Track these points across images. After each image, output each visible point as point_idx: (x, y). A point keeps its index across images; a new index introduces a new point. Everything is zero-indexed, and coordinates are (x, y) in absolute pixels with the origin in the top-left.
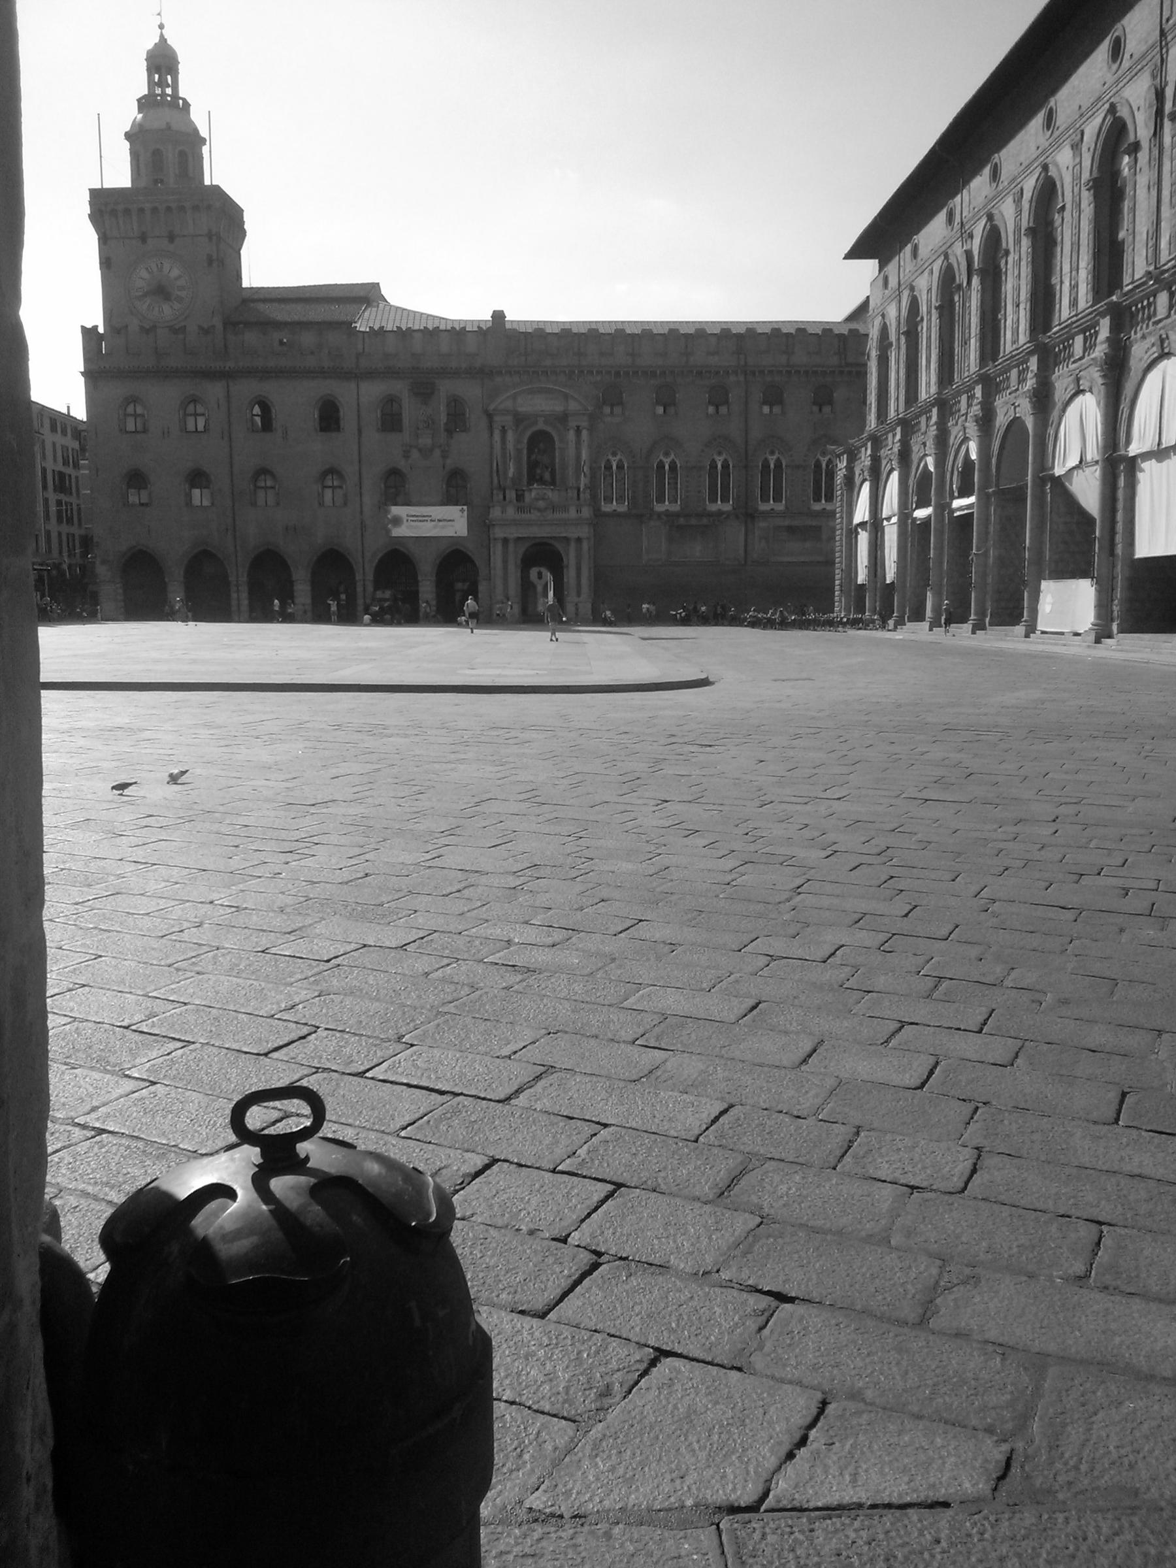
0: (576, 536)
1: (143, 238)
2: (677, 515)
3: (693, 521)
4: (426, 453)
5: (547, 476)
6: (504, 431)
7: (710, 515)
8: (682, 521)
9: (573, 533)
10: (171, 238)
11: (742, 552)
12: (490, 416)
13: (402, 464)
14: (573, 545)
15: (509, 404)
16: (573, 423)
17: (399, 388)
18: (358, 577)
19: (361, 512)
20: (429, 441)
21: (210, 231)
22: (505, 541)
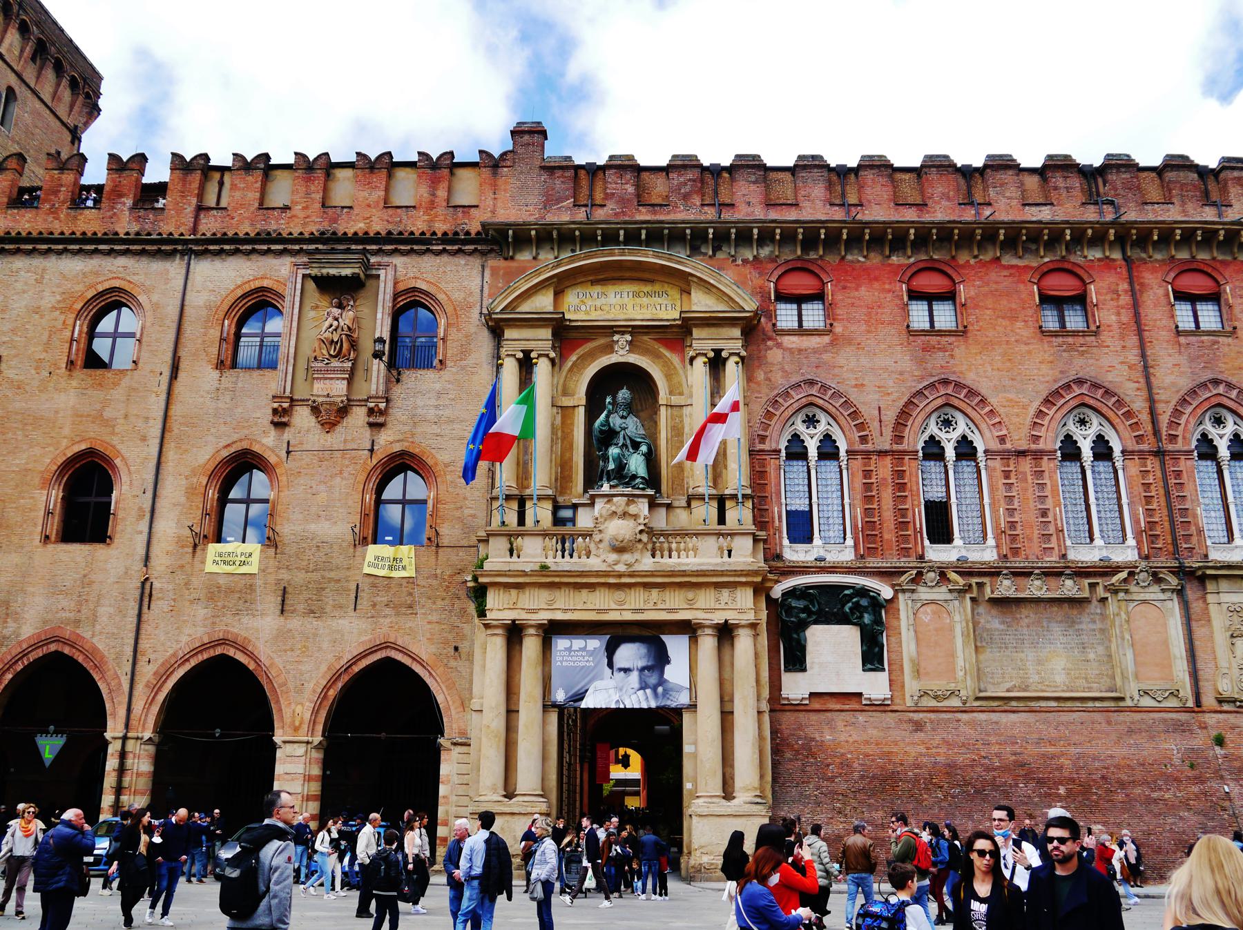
0: (719, 618)
2: (993, 572)
3: (1036, 588)
4: (332, 415)
5: (637, 464)
6: (526, 364)
7: (1081, 572)
8: (1006, 587)
9: (708, 608)
11: (1181, 669)
12: (496, 329)
13: (268, 442)
14: (708, 643)
15: (544, 302)
16: (704, 341)
17: (280, 272)
18: (113, 730)
19: (147, 558)
20: (338, 388)
22: (514, 633)
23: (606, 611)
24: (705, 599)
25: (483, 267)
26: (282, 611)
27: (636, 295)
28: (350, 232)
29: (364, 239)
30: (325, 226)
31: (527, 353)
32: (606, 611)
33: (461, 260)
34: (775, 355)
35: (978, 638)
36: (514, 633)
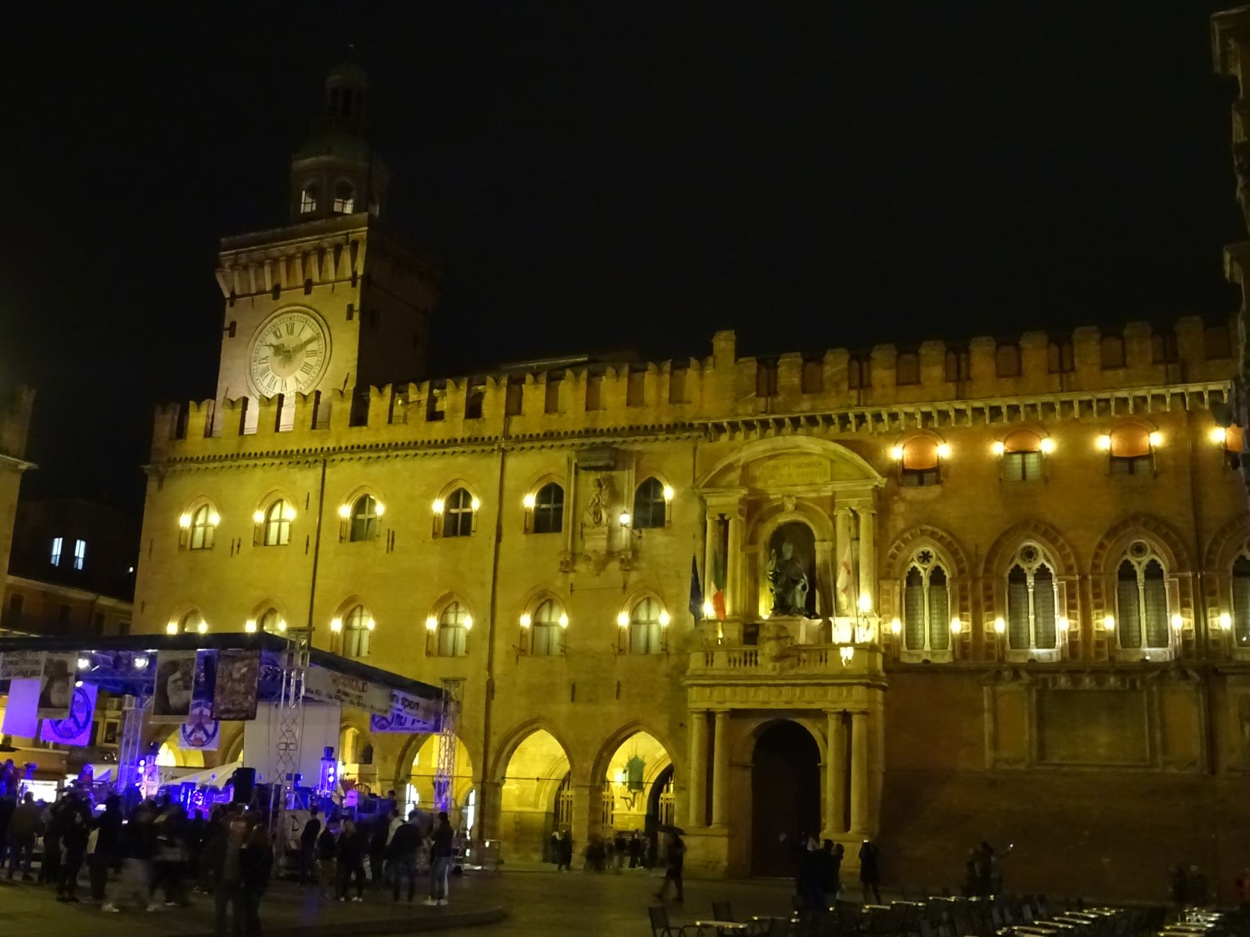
0: (840, 707)
1: (276, 291)
8: (1063, 682)
9: (832, 701)
10: (308, 286)
21: (355, 274)
23: (768, 703)
24: (832, 692)
25: (695, 449)
26: (573, 700)
27: (799, 466)
28: (605, 428)
29: (615, 432)
30: (588, 425)
31: (722, 516)
32: (768, 703)
33: (679, 444)
34: (900, 508)
35: (1042, 720)
36: (710, 716)
